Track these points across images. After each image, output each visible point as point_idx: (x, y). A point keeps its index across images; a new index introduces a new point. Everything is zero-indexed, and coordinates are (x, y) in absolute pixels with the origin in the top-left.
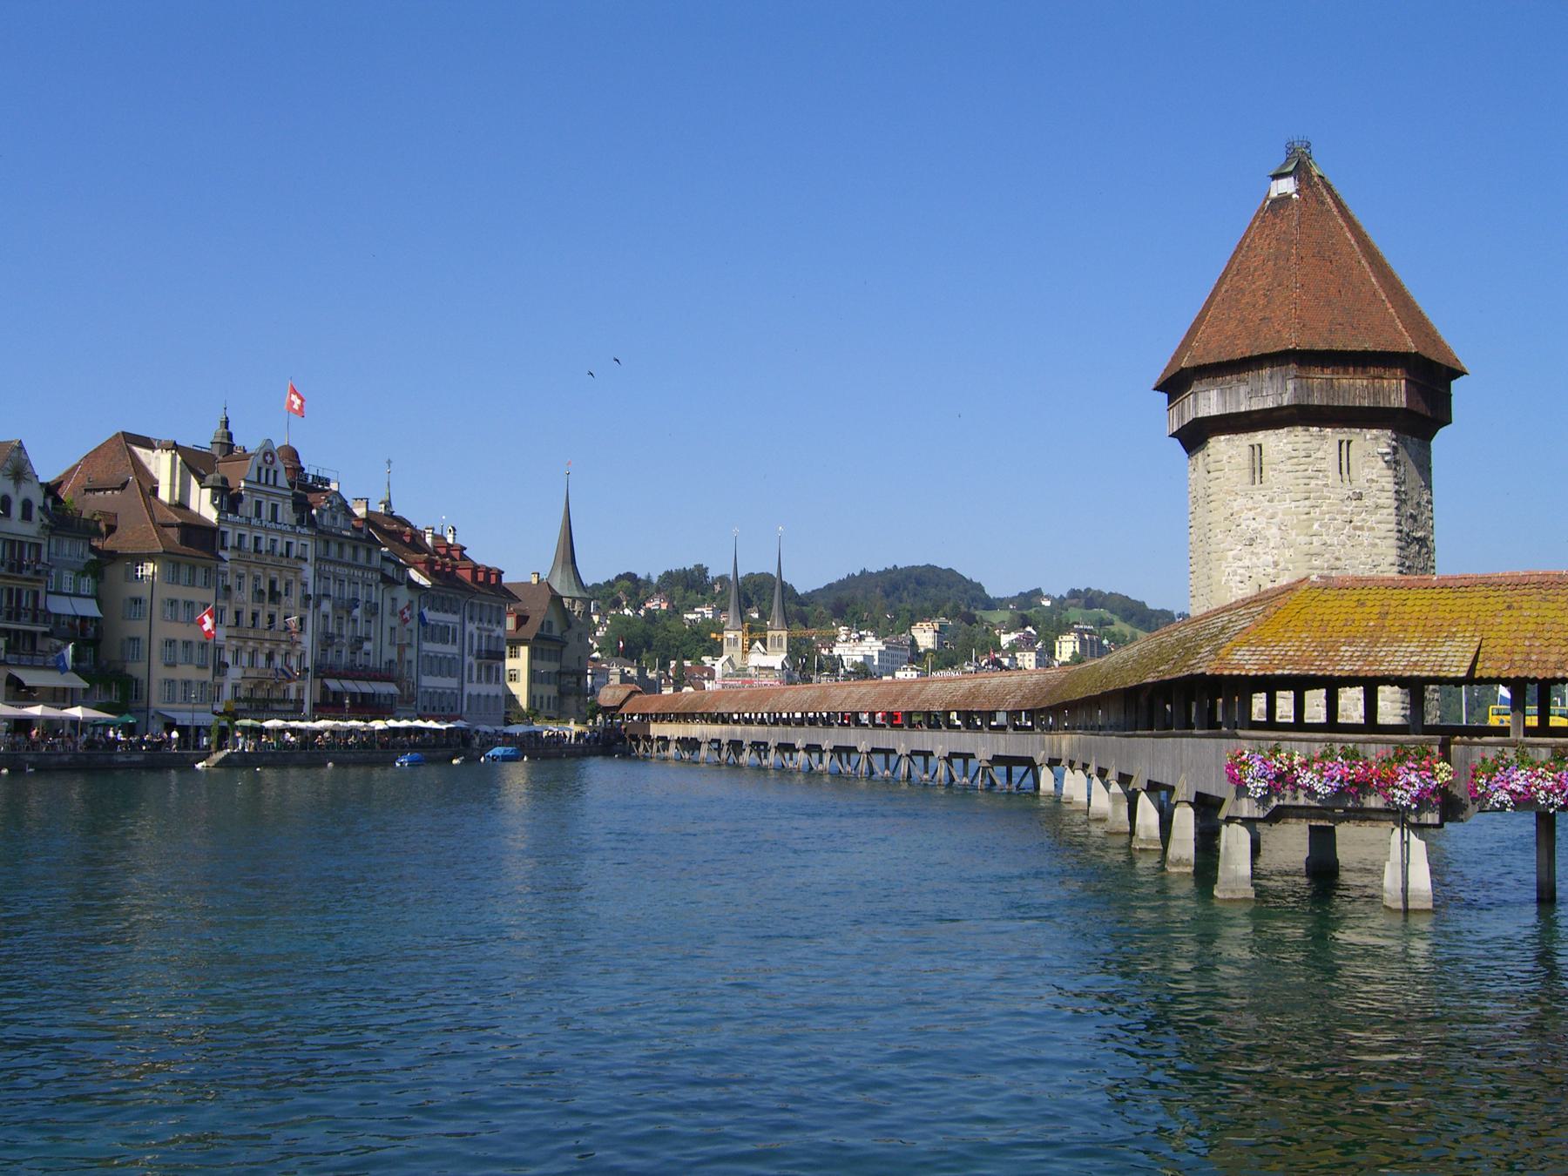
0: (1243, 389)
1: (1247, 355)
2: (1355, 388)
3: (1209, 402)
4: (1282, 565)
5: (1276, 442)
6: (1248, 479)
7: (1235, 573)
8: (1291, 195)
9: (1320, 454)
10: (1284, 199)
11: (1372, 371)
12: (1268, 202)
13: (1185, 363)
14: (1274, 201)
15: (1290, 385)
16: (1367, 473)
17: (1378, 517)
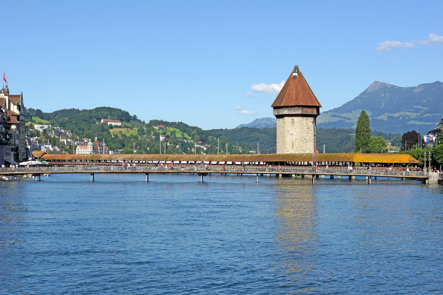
0: (292, 110)
1: (294, 105)
2: (309, 111)
3: (286, 112)
4: (297, 139)
5: (296, 119)
6: (291, 125)
7: (289, 140)
8: (296, 76)
9: (303, 121)
10: (295, 77)
11: (312, 108)
12: (292, 76)
13: (282, 105)
14: (294, 76)
15: (300, 110)
16: (310, 124)
17: (311, 132)
